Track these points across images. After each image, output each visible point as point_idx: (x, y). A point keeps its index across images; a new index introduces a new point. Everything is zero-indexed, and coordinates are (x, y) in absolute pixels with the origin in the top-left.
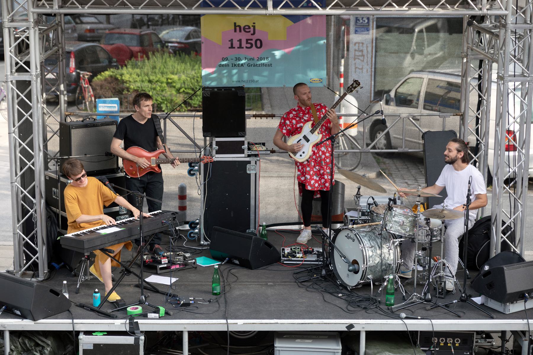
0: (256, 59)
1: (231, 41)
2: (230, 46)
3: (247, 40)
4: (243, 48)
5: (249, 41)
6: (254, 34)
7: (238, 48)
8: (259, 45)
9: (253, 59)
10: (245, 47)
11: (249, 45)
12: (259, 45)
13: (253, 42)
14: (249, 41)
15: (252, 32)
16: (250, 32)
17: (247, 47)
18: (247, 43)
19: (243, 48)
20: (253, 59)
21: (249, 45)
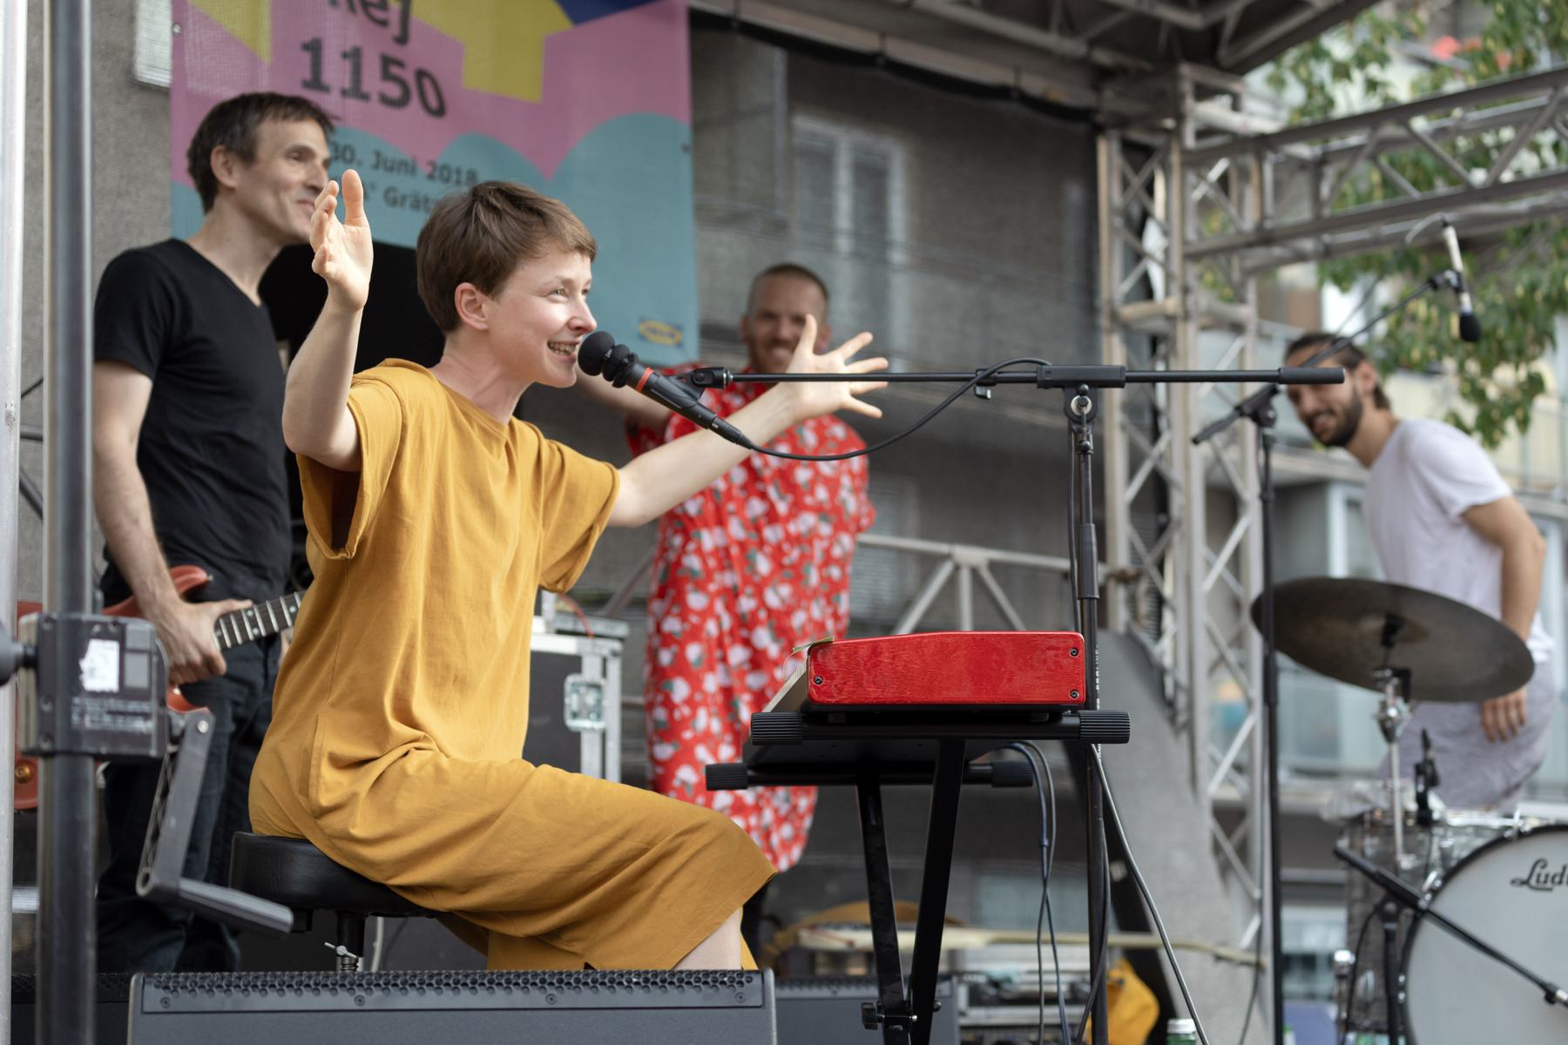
0: (423, 170)
1: (314, 48)
2: (307, 74)
3: (387, 61)
4: (365, 97)
5: (395, 70)
6: (402, 39)
7: (344, 93)
8: (433, 102)
9: (407, 167)
10: (375, 98)
11: (394, 91)
12: (433, 102)
13: (409, 76)
14: (395, 70)
15: (395, 29)
16: (383, 23)
17: (386, 101)
18: (386, 76)
19: (365, 97)
20: (407, 167)
21: (394, 91)
